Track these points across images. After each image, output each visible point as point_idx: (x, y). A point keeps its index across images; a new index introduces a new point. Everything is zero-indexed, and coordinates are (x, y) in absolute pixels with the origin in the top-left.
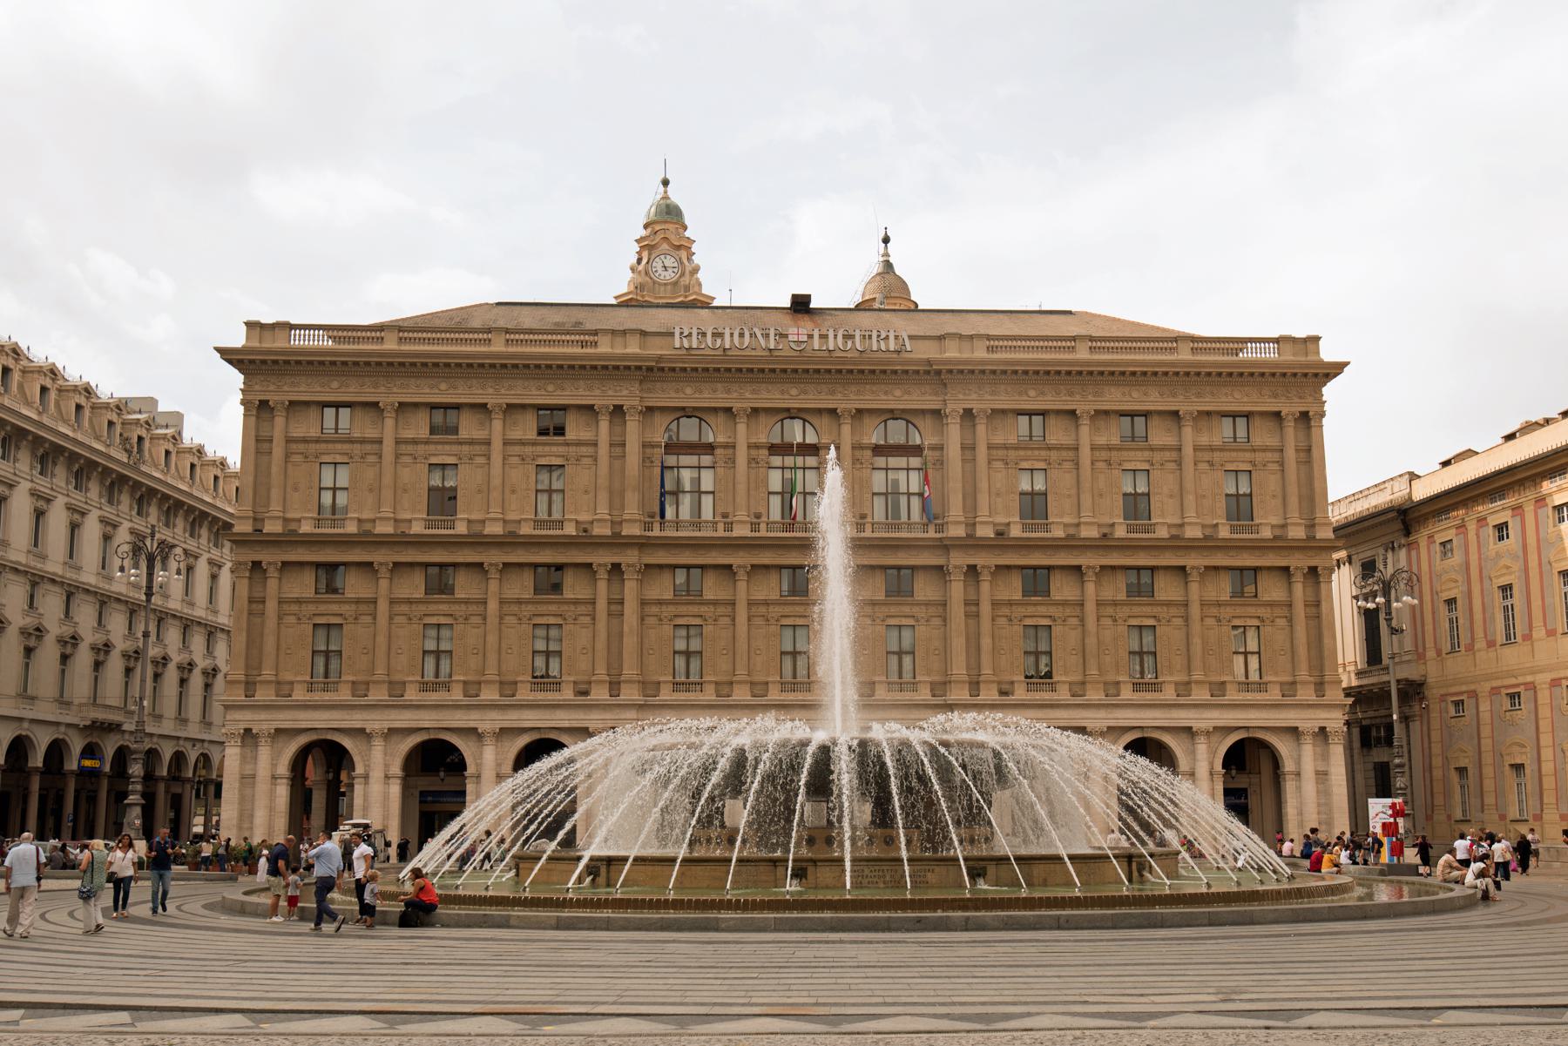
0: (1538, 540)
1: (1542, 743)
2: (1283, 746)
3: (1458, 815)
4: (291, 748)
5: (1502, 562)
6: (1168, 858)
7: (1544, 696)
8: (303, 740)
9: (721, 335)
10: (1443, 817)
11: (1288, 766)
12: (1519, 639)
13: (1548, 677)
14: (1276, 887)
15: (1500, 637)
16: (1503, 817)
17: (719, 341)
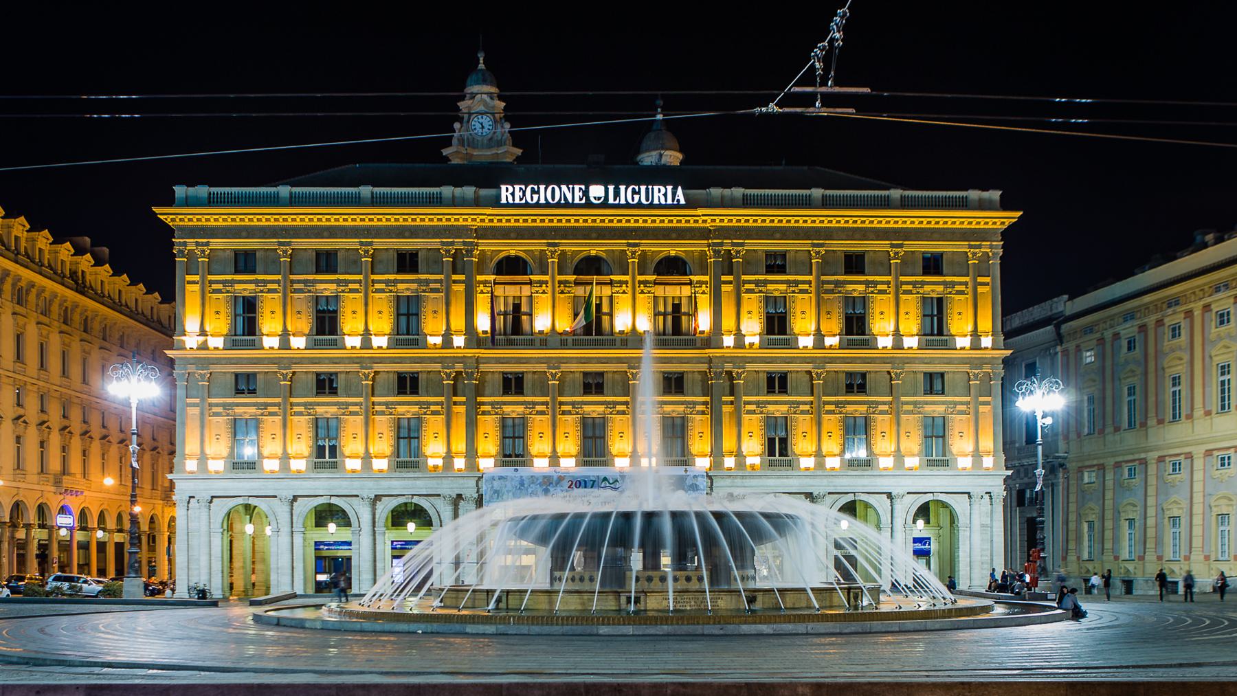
0: (1156, 352)
1: (1149, 504)
2: (959, 505)
3: (1086, 556)
4: (221, 508)
5: (1129, 368)
6: (876, 592)
7: (1152, 469)
8: (232, 503)
9: (538, 192)
10: (1074, 558)
11: (962, 520)
12: (1138, 426)
13: (1156, 454)
14: (943, 607)
15: (1125, 425)
16: (1116, 558)
17: (536, 197)
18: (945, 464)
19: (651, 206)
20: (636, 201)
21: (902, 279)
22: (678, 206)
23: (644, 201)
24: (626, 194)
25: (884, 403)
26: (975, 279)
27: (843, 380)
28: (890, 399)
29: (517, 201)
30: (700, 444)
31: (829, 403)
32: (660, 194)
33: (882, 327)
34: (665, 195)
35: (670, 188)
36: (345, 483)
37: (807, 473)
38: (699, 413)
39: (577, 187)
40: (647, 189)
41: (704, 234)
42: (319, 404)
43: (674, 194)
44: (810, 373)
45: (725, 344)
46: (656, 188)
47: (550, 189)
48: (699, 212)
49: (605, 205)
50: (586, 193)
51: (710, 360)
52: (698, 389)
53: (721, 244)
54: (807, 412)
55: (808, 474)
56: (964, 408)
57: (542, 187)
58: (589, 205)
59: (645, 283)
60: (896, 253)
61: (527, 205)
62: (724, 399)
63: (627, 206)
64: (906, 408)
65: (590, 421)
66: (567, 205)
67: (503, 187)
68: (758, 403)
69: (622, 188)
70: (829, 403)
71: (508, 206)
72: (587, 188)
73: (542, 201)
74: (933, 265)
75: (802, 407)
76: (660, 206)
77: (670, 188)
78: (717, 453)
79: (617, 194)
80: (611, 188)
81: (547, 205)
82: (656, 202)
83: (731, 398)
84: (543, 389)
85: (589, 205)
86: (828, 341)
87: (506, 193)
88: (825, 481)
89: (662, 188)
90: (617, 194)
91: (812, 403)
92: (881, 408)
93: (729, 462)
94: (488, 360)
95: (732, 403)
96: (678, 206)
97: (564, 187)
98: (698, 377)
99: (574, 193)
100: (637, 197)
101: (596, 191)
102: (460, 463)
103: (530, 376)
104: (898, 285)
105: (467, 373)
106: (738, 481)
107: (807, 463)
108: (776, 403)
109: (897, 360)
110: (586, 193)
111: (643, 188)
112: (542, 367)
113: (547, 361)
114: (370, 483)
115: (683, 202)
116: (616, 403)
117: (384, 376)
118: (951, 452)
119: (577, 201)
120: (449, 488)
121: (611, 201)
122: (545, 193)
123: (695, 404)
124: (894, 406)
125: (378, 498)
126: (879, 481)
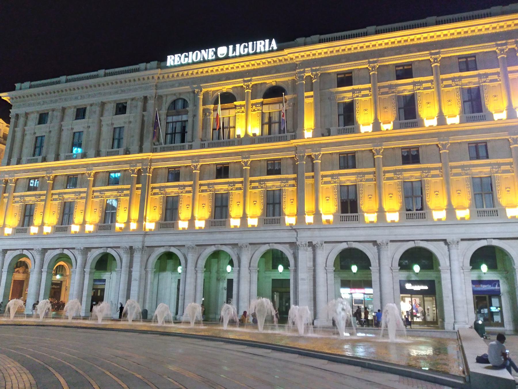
9: (188, 57)
18: (495, 213)
19: (256, 53)
20: (246, 52)
21: (443, 76)
22: (272, 51)
23: (251, 52)
24: (240, 49)
25: (435, 169)
26: (506, 69)
27: (399, 154)
28: (439, 165)
29: (176, 63)
30: (289, 208)
31: (389, 172)
32: (262, 45)
33: (428, 114)
34: (264, 46)
35: (267, 41)
36: (70, 240)
37: (371, 225)
38: (290, 186)
39: (210, 50)
40: (253, 44)
41: (292, 67)
42: (65, 193)
43: (270, 44)
44: (371, 151)
45: (306, 137)
46: (258, 42)
47: (195, 53)
48: (286, 51)
49: (227, 57)
50: (216, 53)
51: (296, 148)
52: (291, 169)
53: (304, 72)
54: (371, 180)
55: (372, 226)
56: (508, 167)
57: (191, 53)
58: (217, 59)
59: (256, 104)
60: (435, 59)
61: (182, 65)
62: (307, 174)
63: (241, 56)
64: (455, 171)
65: (220, 196)
66: (204, 61)
67: (169, 57)
68: (332, 176)
69: (238, 46)
70: (389, 172)
71: (171, 67)
72: (216, 50)
73: (190, 61)
74: (468, 64)
75: (367, 177)
76: (261, 53)
77: (267, 41)
78: (300, 213)
79: (234, 50)
80: (231, 47)
81: (194, 63)
82: (258, 51)
83: (312, 174)
84: (191, 176)
85: (217, 59)
86: (384, 127)
87: (172, 60)
88: (387, 231)
89: (262, 42)
90: (234, 50)
91: (374, 173)
92: (433, 172)
93: (309, 219)
94: (157, 160)
95: (313, 177)
96: (272, 51)
97: (203, 51)
98: (290, 162)
99: (208, 54)
100: (246, 50)
101: (222, 51)
102: (133, 226)
103: (183, 169)
104: (438, 82)
105: (143, 169)
106: (317, 233)
107: (371, 217)
108: (346, 174)
109: (442, 133)
110: (216, 53)
111: (250, 44)
112: (188, 163)
113: (191, 158)
114: (83, 240)
115: (275, 48)
116: (234, 183)
117: (101, 174)
118: (500, 205)
119: (210, 58)
120: (125, 242)
121: (230, 55)
122: (193, 56)
123: (287, 180)
124: (443, 170)
125: (88, 249)
126: (435, 230)
